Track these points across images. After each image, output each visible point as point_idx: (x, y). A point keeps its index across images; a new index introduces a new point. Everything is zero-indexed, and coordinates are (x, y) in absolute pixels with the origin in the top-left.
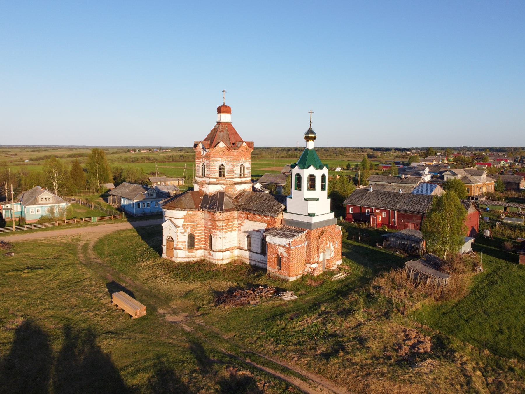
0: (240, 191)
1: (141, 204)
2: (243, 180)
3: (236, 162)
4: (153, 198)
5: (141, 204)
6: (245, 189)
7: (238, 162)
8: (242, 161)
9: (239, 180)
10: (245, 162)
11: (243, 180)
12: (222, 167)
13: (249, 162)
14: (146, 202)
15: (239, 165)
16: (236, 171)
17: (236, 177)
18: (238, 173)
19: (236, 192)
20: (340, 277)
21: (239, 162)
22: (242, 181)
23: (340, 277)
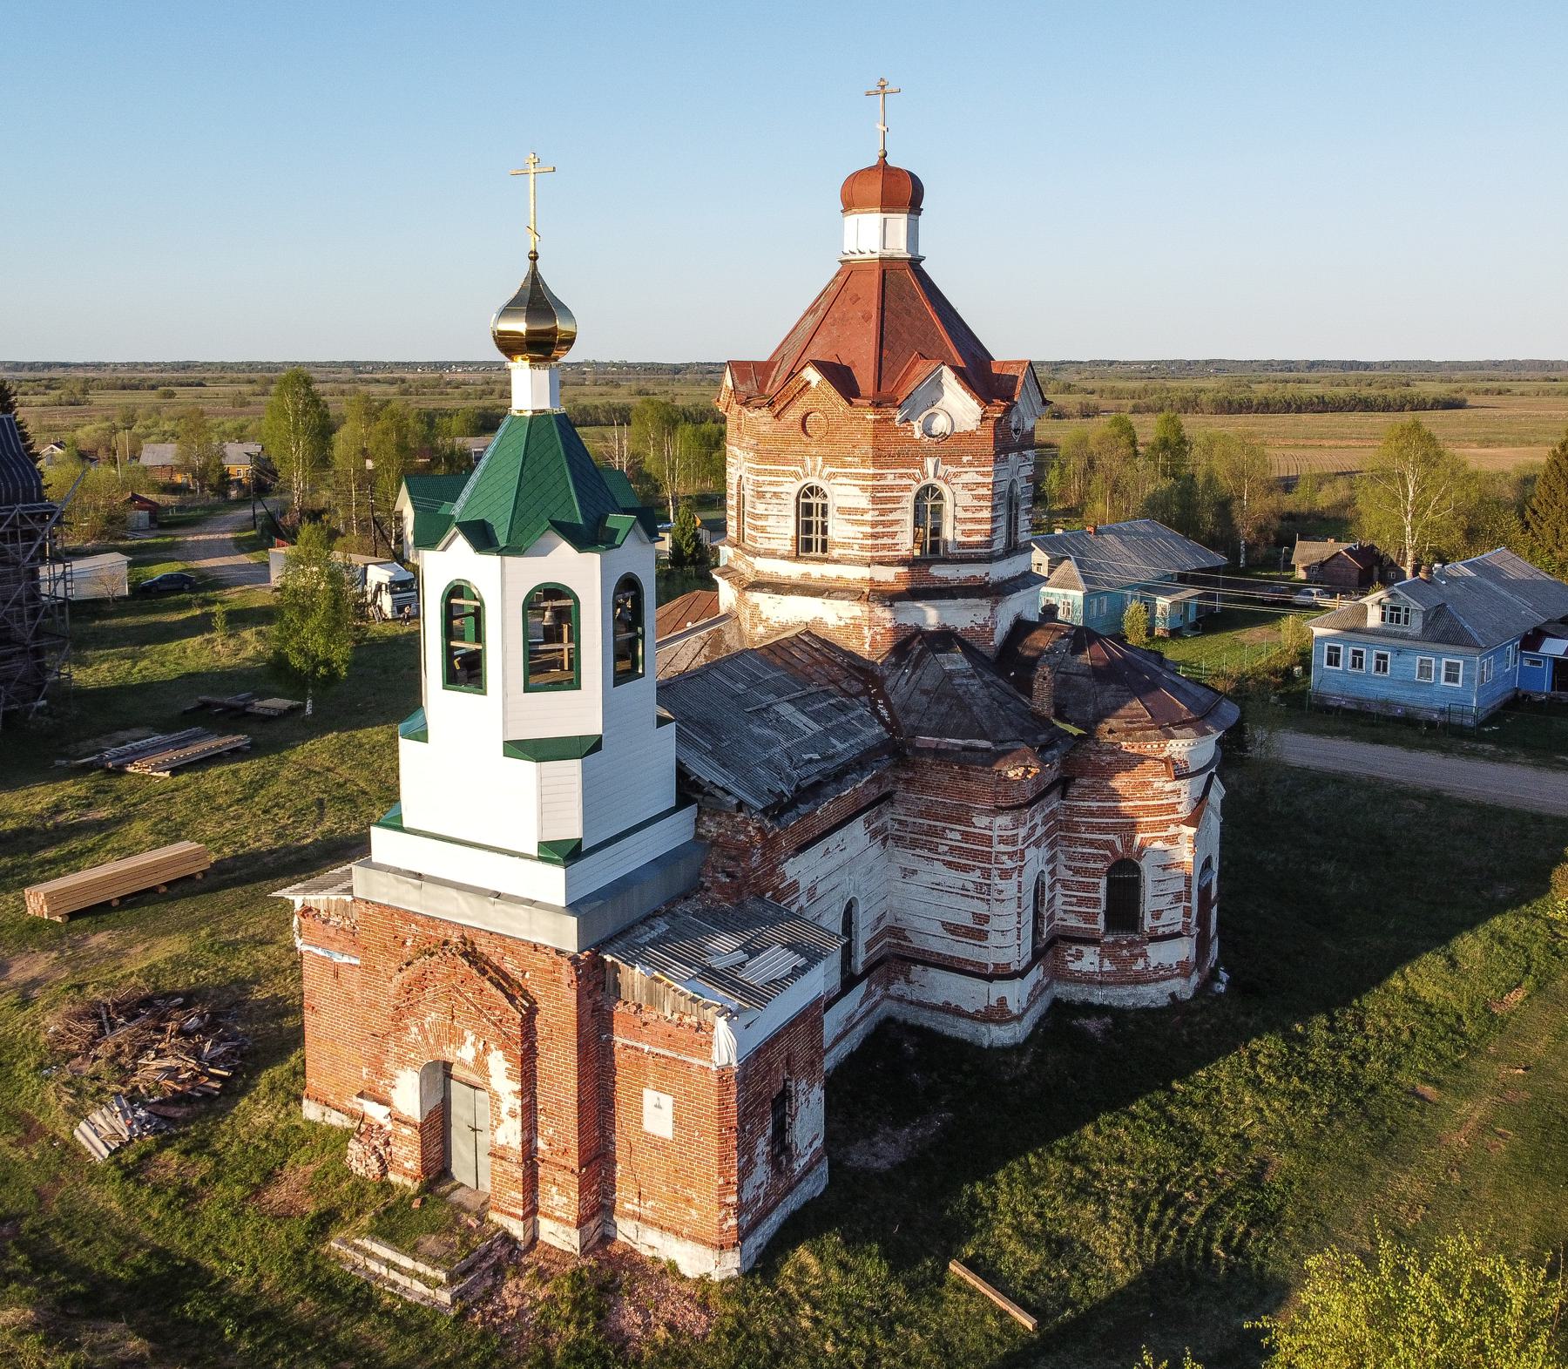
0: (785, 629)
1: (1346, 654)
2: (817, 571)
3: (771, 473)
4: (1404, 636)
5: (1346, 654)
6: (819, 622)
7: (784, 473)
8: (815, 471)
9: (792, 571)
10: (832, 475)
11: (817, 571)
12: (813, 500)
13: (857, 476)
14: (1348, 642)
15: (792, 488)
16: (771, 521)
17: (771, 554)
18: (784, 529)
19: (761, 630)
20: (404, 1281)
21: (796, 475)
22: (807, 576)
23: (404, 1281)
